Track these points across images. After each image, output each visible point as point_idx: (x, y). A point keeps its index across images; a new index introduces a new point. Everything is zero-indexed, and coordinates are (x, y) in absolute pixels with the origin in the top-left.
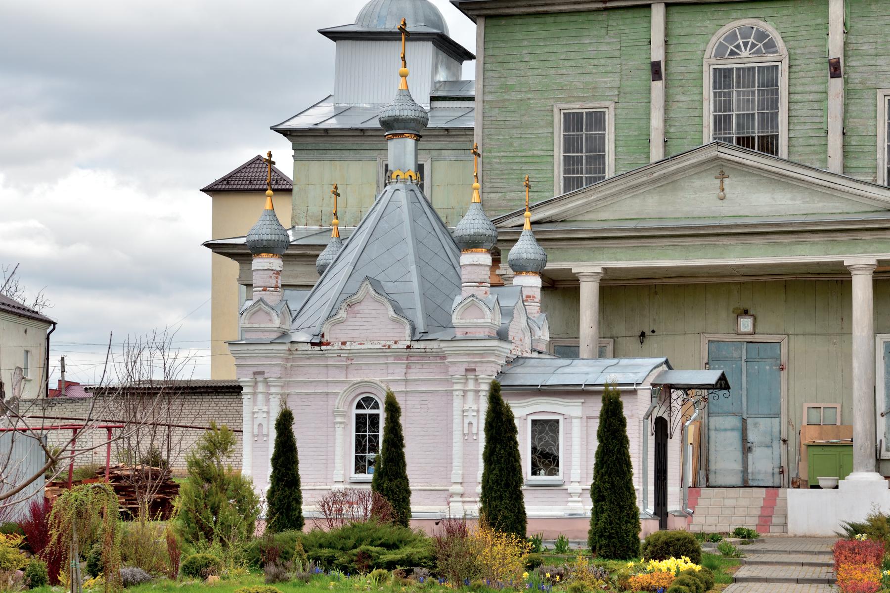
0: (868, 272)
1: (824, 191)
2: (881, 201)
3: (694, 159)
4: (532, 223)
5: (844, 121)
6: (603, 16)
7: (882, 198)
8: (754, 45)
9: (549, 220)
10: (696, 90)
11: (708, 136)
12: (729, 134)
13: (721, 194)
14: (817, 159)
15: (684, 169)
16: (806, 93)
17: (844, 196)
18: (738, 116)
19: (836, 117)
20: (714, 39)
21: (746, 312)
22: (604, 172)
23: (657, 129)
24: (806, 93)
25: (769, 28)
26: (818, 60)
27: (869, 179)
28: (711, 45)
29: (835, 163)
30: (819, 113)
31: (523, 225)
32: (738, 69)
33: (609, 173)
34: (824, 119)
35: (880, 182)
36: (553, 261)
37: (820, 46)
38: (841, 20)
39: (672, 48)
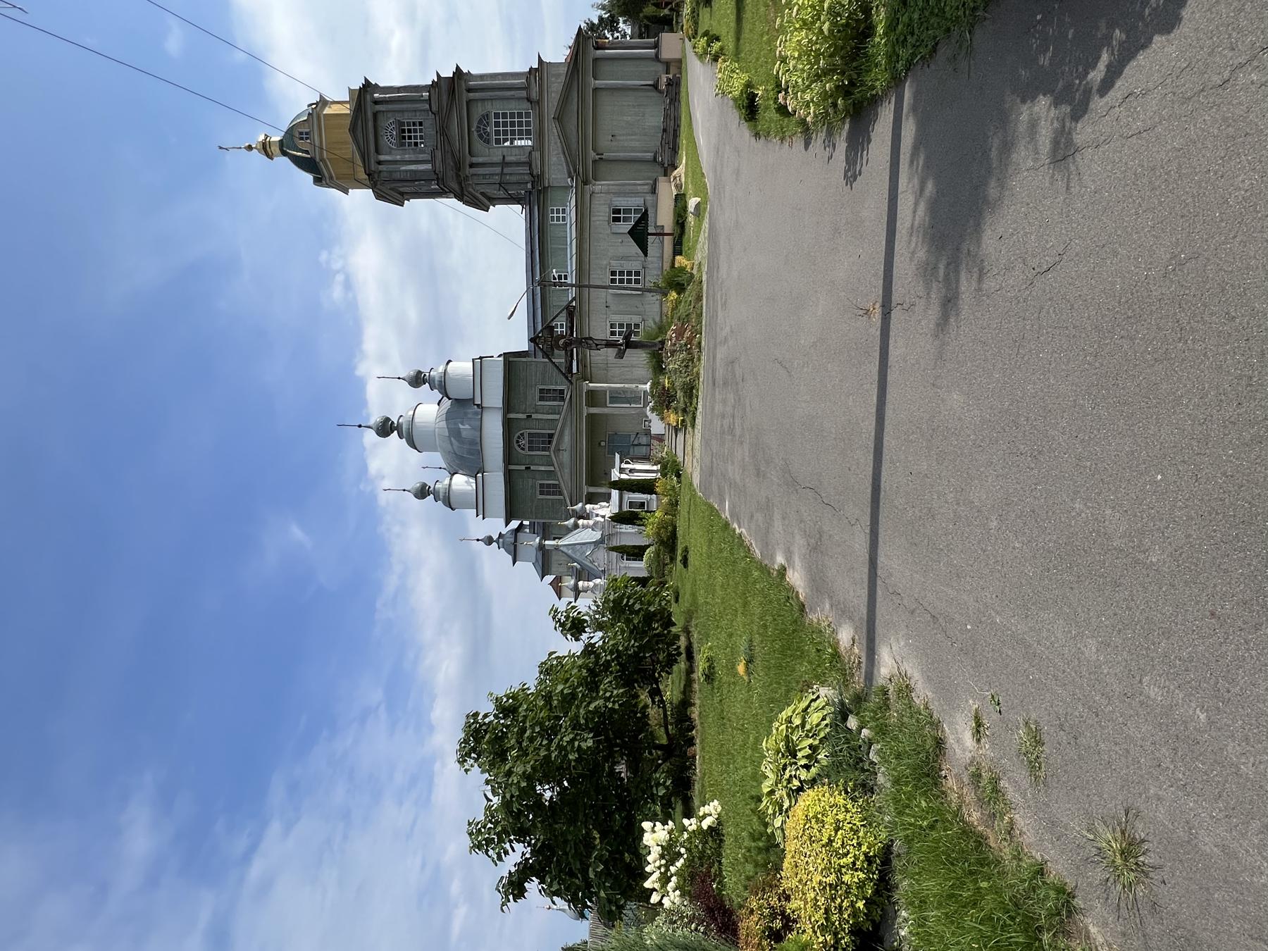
11: (547, 453)
21: (600, 444)
25: (517, 435)
29: (557, 417)
33: (557, 482)
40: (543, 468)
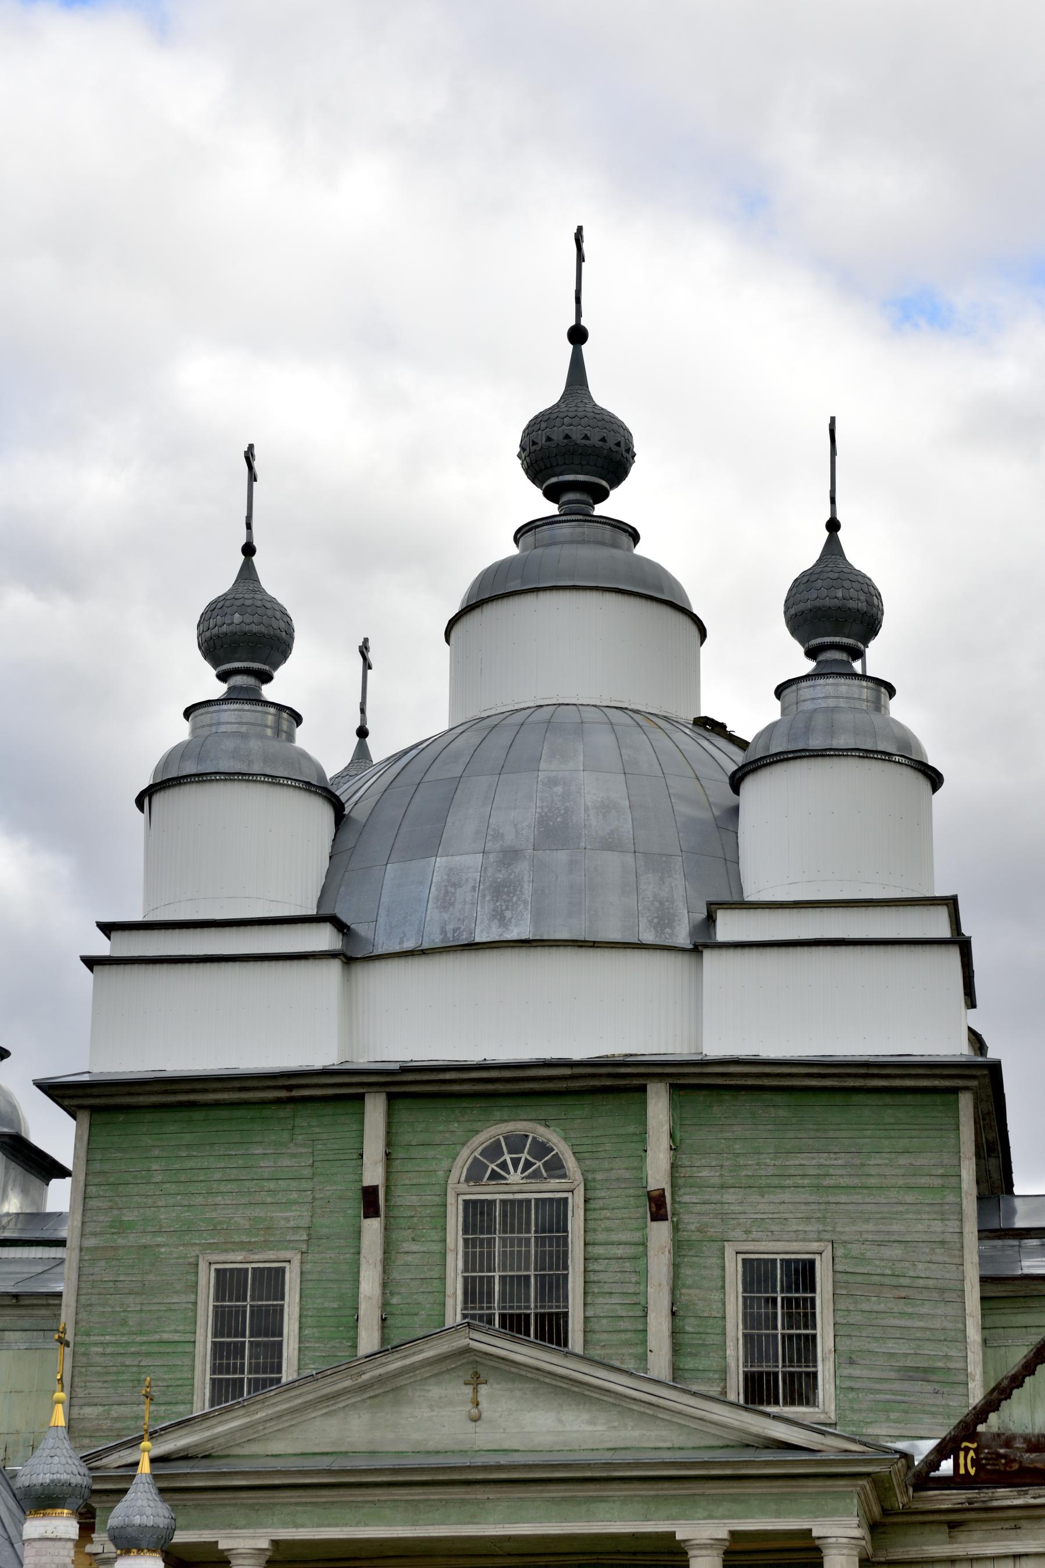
0: (715, 1552)
1: (642, 1410)
2: (733, 1428)
3: (430, 1351)
4: (153, 1461)
5: (674, 1290)
6: (287, 1111)
7: (736, 1424)
8: (528, 1165)
9: (182, 1454)
10: (435, 1235)
11: (454, 1312)
12: (489, 1308)
13: (474, 1411)
14: (631, 1354)
15: (412, 1368)
16: (612, 1243)
17: (675, 1420)
18: (503, 1278)
19: (660, 1285)
20: (465, 1152)
22: (280, 1371)
23: (370, 1298)
24: (612, 1243)
25: (552, 1137)
26: (631, 1191)
27: (714, 1390)
28: (459, 1162)
29: (660, 1363)
30: (634, 1278)
31: (136, 1464)
32: (504, 1202)
33: (288, 1373)
34: (642, 1288)
35: (732, 1397)
36: (186, 1528)
37: (633, 1169)
38: (666, 1128)
39: (397, 1165)
40: (369, 1284)
